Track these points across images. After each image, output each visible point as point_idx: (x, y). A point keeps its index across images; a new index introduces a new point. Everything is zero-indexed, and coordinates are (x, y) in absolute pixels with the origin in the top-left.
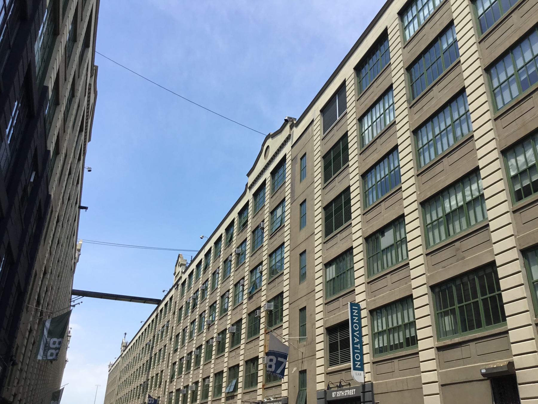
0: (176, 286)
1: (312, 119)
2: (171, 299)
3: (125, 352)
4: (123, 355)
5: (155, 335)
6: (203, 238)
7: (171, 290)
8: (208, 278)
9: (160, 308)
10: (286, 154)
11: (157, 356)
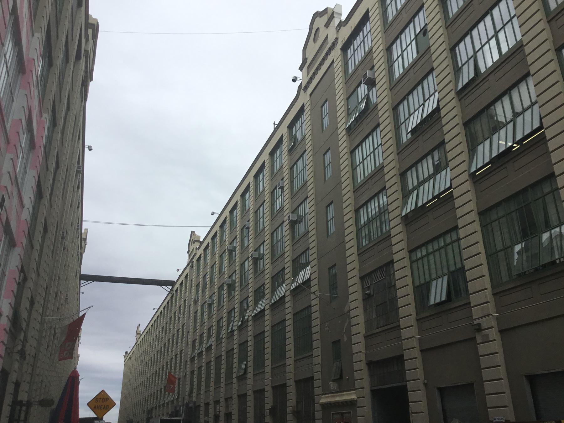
1: (332, 61)
2: (186, 277)
3: (141, 339)
4: (139, 342)
5: (181, 306)
7: (185, 269)
8: (237, 236)
9: (175, 289)
10: (368, 9)
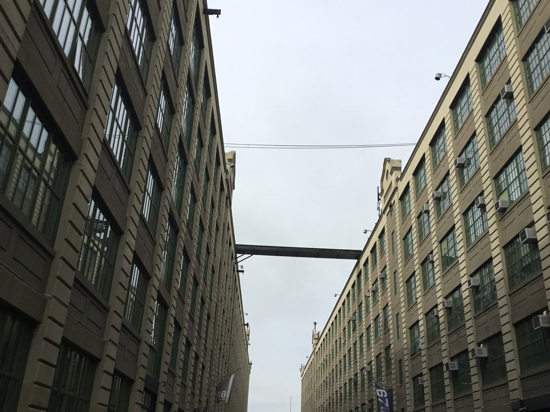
0: (388, 210)
3: (319, 345)
4: (317, 349)
6: (367, 232)
11: (352, 352)
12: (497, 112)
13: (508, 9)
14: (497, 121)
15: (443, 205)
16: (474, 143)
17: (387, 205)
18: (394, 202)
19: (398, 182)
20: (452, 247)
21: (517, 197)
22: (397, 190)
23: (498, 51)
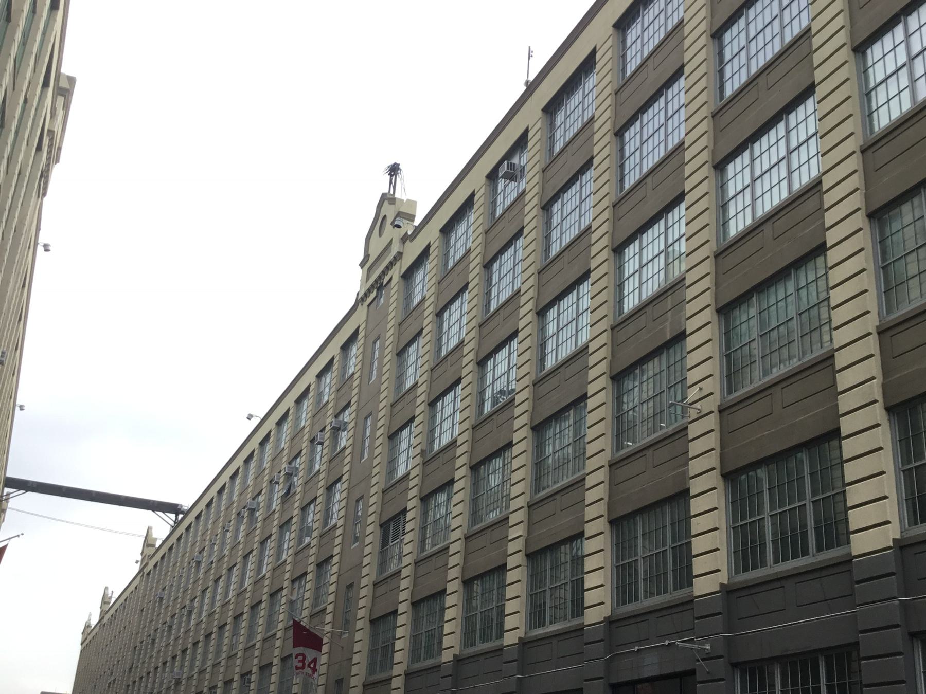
3: (157, 558)
4: (150, 566)
12: (581, 188)
13: (609, 43)
14: (559, 221)
15: (448, 341)
16: (503, 263)
17: (372, 286)
18: (391, 279)
19: (404, 243)
20: (450, 416)
21: (569, 351)
22: (401, 258)
23: (581, 105)
